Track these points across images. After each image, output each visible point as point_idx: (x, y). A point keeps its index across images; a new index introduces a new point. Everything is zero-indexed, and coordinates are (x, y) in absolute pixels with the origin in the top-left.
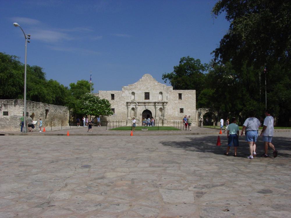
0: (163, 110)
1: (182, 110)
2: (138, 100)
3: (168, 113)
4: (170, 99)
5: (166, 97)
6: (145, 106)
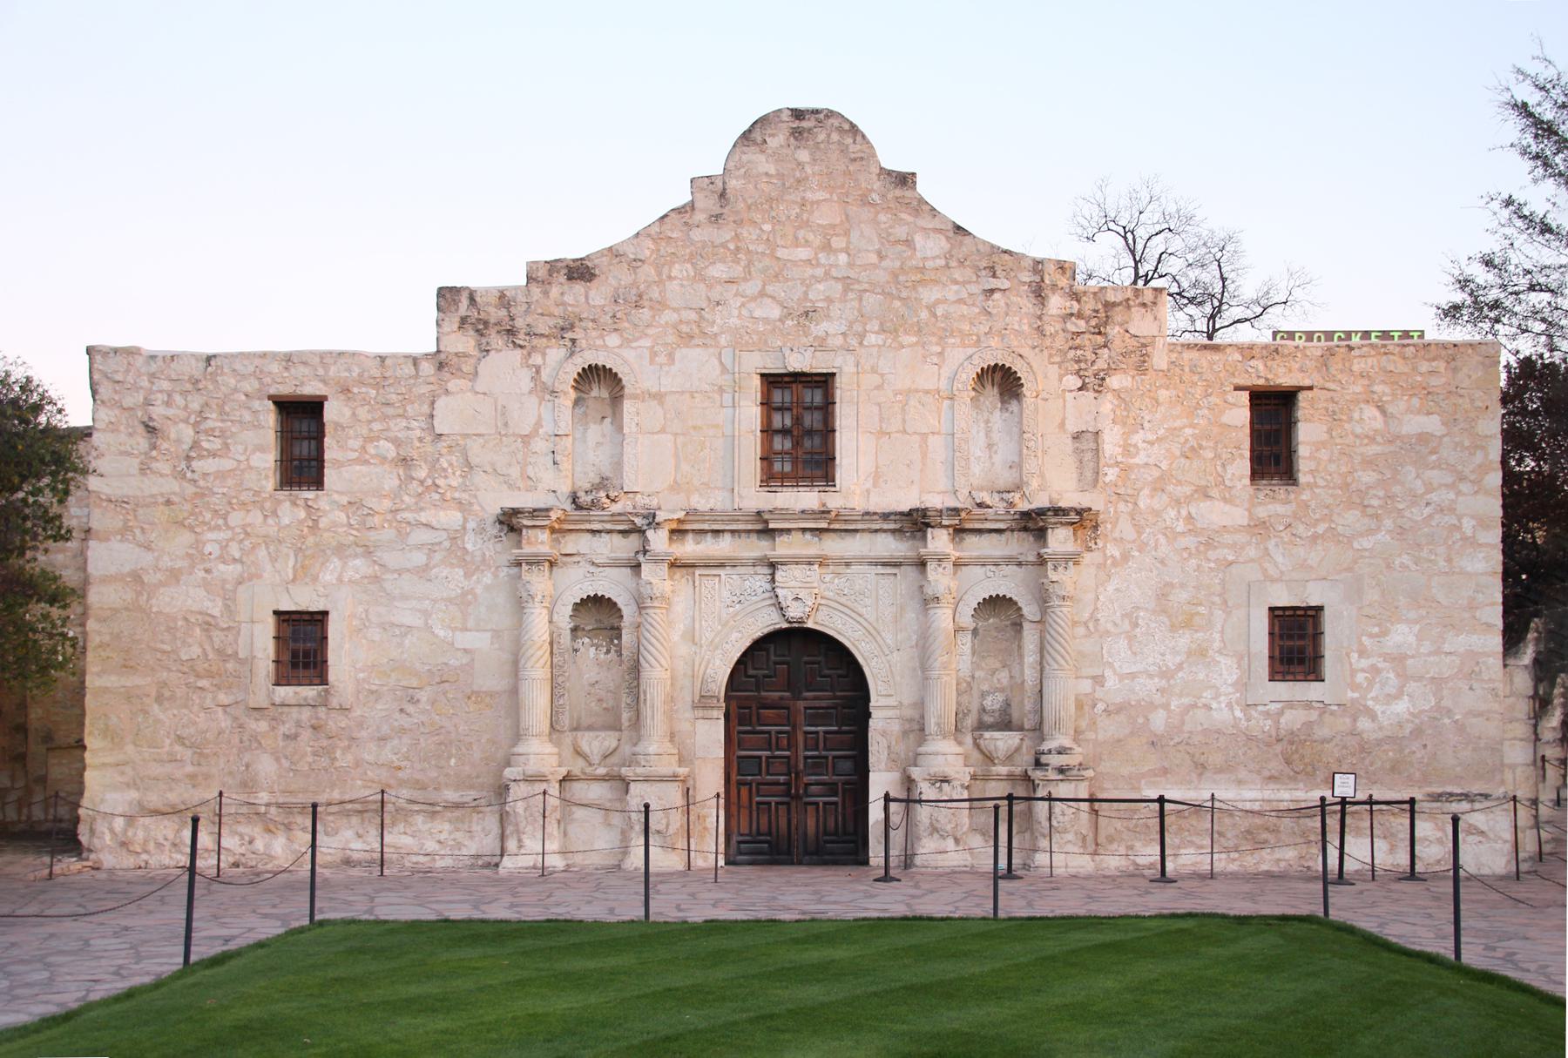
0: (1030, 636)
2: (675, 487)
3: (1099, 680)
4: (1126, 470)
5: (1077, 437)
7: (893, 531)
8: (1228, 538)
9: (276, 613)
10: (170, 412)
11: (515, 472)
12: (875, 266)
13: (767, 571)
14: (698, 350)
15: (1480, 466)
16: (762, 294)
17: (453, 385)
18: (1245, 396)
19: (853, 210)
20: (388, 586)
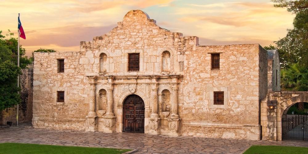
1: (219, 98)
2: (114, 72)
3: (183, 104)
5: (180, 62)
6: (129, 84)
7: (149, 79)
8: (207, 80)
9: (57, 91)
10: (44, 62)
11: (91, 70)
12: (146, 35)
13: (128, 85)
14: (118, 50)
15: (254, 66)
16: (128, 40)
17: (82, 56)
18: (210, 54)
19: (142, 26)
20: (73, 87)
